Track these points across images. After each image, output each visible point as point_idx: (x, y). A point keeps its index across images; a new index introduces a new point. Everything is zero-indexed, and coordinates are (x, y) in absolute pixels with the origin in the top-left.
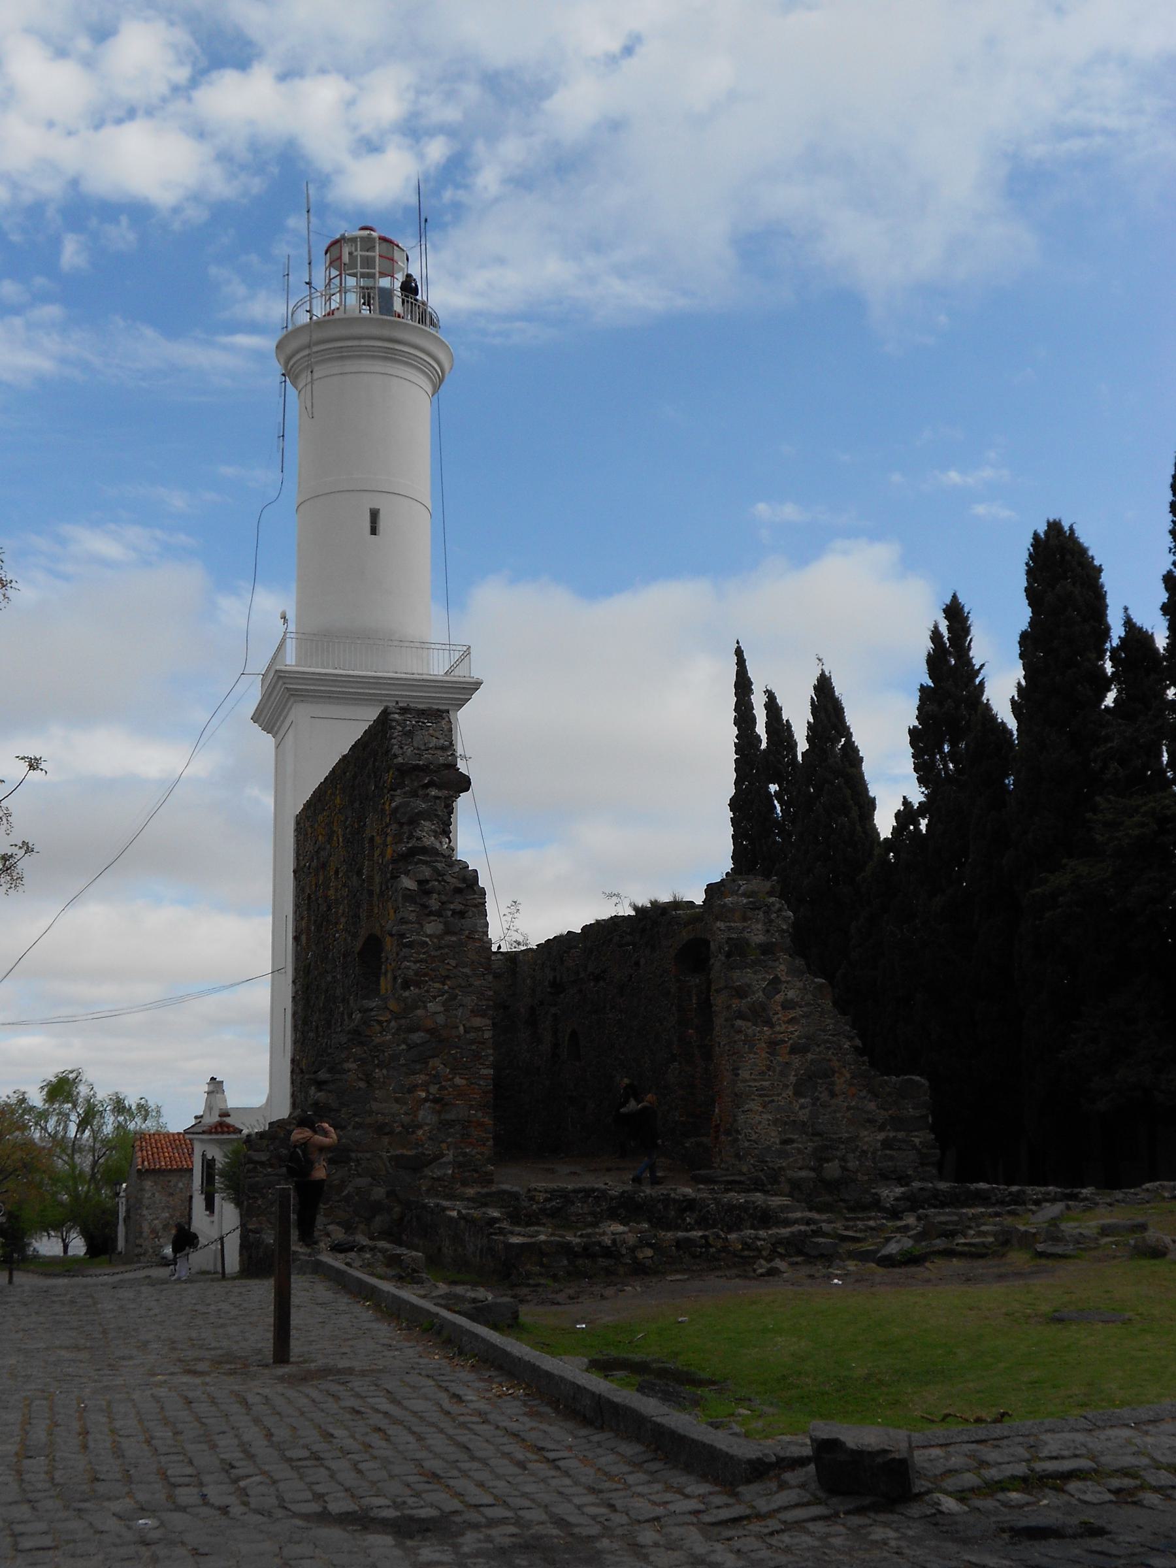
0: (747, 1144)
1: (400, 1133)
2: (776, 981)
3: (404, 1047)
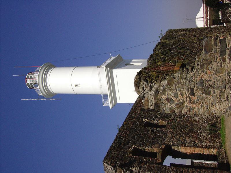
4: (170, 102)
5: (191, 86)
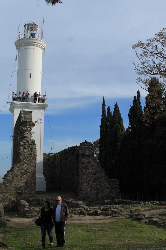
0: (83, 191)
1: (19, 188)
2: (90, 161)
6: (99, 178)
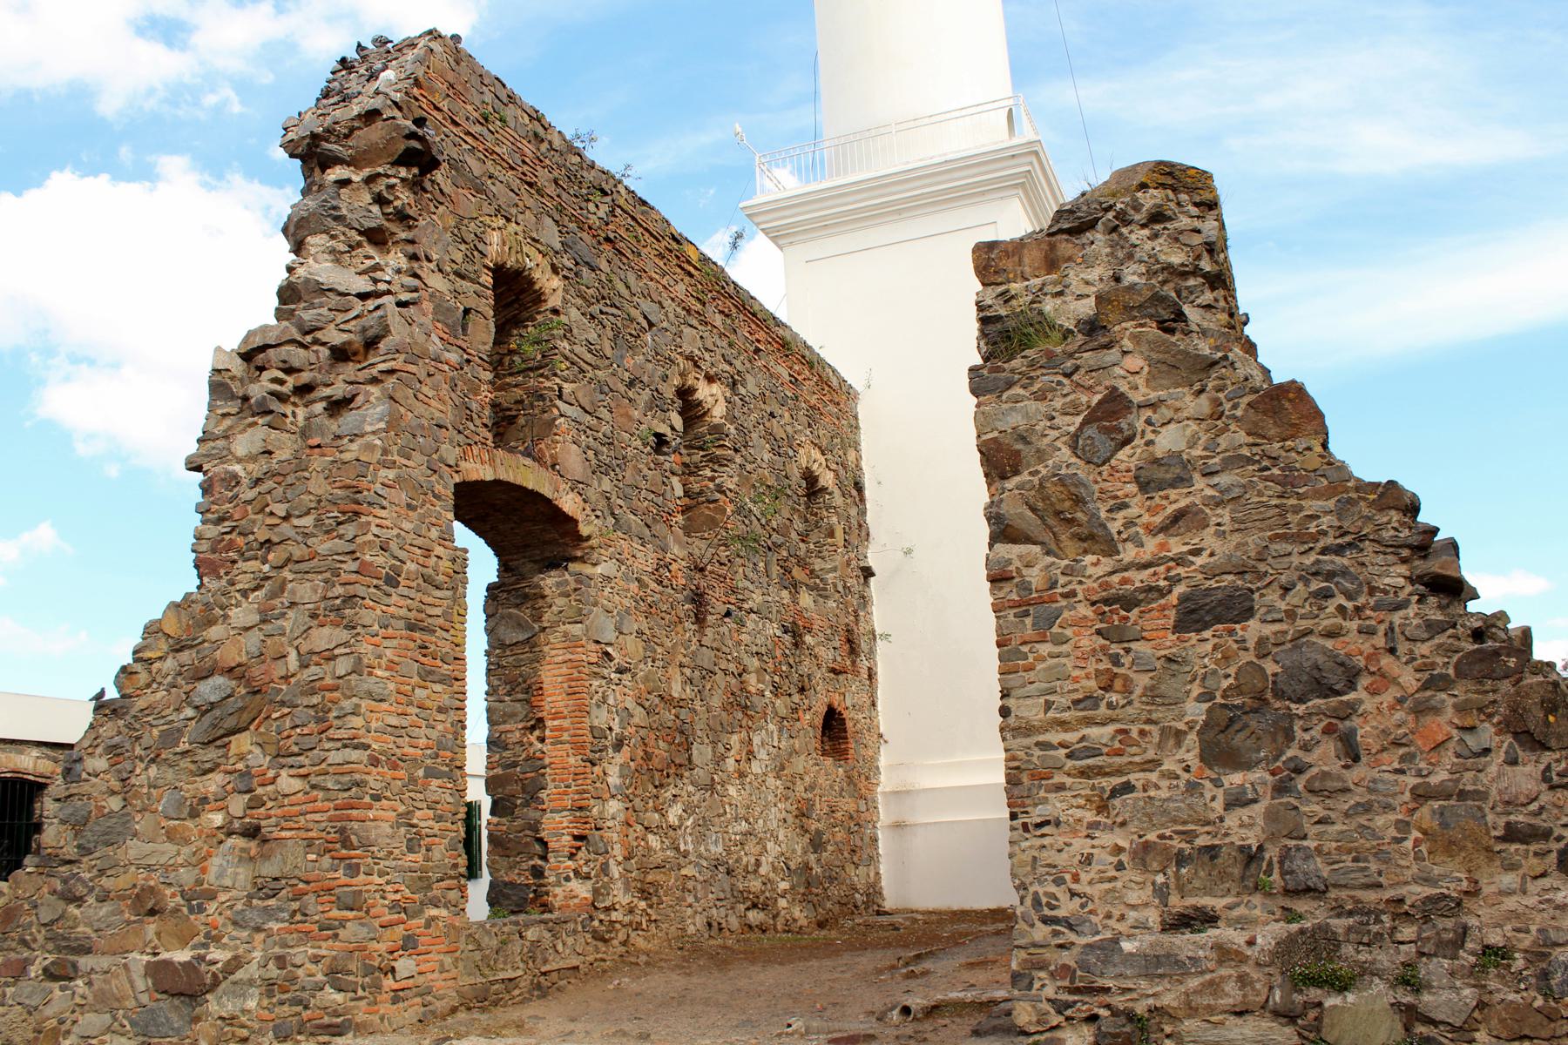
0: (1041, 932)
1: (176, 910)
3: (189, 712)
4: (1091, 431)
5: (1273, 596)
6: (1330, 681)
